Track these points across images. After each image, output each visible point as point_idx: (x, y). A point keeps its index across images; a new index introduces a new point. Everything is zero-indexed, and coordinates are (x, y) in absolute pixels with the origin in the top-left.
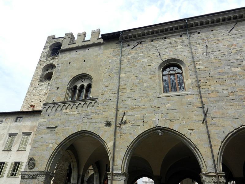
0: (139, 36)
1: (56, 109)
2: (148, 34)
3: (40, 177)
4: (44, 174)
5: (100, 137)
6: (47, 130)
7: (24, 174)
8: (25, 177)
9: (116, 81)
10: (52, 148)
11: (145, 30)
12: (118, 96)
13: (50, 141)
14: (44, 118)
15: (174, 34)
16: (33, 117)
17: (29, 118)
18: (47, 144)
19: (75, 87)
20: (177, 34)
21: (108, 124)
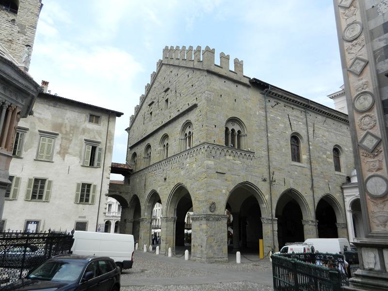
0: (279, 96)
2: (285, 98)
4: (226, 218)
6: (216, 174)
9: (265, 139)
12: (269, 155)
13: (222, 187)
15: (298, 108)
16: (54, 107)
17: (47, 106)
19: (227, 129)
20: (300, 109)
21: (265, 180)
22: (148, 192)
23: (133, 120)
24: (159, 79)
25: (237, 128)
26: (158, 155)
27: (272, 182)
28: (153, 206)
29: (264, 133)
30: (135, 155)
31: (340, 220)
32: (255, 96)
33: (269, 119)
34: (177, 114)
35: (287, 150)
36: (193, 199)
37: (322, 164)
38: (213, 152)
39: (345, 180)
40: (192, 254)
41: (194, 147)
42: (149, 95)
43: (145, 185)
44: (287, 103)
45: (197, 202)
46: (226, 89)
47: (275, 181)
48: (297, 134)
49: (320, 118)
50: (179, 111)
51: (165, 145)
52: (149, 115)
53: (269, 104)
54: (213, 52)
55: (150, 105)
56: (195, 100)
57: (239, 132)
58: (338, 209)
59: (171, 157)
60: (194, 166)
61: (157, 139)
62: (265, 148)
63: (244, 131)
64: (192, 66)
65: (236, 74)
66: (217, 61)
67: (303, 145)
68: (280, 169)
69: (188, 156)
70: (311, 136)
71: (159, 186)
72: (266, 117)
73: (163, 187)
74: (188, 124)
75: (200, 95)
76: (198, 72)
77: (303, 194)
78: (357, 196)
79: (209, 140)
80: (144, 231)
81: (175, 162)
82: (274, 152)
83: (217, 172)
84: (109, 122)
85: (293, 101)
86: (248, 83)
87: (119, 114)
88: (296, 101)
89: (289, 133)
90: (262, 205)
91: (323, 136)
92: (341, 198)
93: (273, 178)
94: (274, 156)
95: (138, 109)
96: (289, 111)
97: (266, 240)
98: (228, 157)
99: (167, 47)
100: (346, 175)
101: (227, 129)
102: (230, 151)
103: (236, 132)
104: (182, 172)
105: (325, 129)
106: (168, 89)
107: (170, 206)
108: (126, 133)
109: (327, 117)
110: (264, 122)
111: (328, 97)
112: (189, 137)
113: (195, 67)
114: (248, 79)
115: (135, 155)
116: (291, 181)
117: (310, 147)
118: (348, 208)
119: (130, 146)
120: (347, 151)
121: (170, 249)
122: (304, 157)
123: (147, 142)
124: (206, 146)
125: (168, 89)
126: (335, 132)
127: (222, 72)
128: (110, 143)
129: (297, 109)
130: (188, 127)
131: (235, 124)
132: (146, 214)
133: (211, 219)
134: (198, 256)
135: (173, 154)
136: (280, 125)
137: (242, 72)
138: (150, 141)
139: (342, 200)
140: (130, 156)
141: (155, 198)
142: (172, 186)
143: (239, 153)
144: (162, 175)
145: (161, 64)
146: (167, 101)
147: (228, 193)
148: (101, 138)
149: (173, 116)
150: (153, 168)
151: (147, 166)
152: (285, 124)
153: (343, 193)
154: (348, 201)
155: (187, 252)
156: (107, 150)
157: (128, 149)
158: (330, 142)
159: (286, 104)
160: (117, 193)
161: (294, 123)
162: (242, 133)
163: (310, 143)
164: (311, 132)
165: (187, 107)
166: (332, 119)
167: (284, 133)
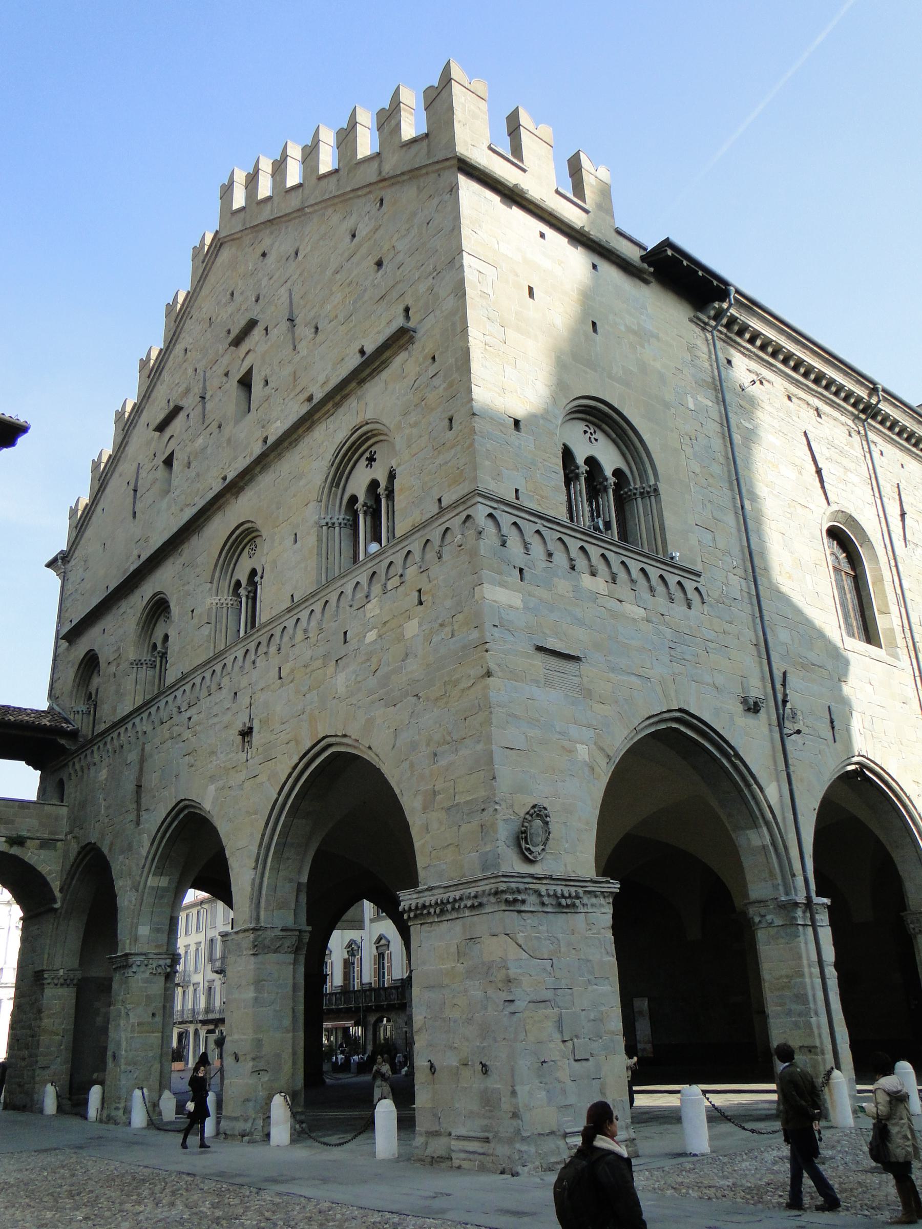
1: (550, 555)
3: (592, 905)
5: (737, 755)
7: (522, 886)
8: (523, 902)
9: (730, 520)
13: (574, 731)
15: (836, 414)
18: (566, 744)
19: (567, 455)
20: (843, 419)
21: (753, 708)
22: (156, 814)
24: (205, 307)
25: (610, 459)
26: (206, 630)
29: (723, 495)
30: (90, 664)
40: (423, 1123)
41: (405, 537)
43: (139, 787)
44: (796, 383)
47: (794, 715)
48: (851, 520)
50: (310, 399)
52: (161, 472)
55: (161, 427)
57: (617, 473)
61: (200, 560)
62: (736, 560)
63: (643, 475)
67: (878, 569)
71: (212, 779)
74: (361, 446)
75: (422, 288)
80: (133, 1020)
81: (300, 635)
83: (540, 649)
93: (785, 702)
98: (586, 580)
101: (567, 455)
102: (594, 552)
104: (341, 681)
106: (252, 324)
107: (276, 870)
108: (53, 580)
110: (717, 444)
115: (90, 664)
121: (279, 1107)
124: (480, 512)
125: (252, 324)
129: (835, 419)
130: (363, 462)
131: (599, 435)
132: (144, 931)
133: (532, 902)
134: (463, 1131)
138: (163, 580)
140: (70, 674)
141: (195, 853)
144: (227, 718)
146: (246, 383)
150: (181, 698)
151: (148, 697)
155: (385, 1111)
159: (793, 389)
162: (635, 484)
167: (800, 510)
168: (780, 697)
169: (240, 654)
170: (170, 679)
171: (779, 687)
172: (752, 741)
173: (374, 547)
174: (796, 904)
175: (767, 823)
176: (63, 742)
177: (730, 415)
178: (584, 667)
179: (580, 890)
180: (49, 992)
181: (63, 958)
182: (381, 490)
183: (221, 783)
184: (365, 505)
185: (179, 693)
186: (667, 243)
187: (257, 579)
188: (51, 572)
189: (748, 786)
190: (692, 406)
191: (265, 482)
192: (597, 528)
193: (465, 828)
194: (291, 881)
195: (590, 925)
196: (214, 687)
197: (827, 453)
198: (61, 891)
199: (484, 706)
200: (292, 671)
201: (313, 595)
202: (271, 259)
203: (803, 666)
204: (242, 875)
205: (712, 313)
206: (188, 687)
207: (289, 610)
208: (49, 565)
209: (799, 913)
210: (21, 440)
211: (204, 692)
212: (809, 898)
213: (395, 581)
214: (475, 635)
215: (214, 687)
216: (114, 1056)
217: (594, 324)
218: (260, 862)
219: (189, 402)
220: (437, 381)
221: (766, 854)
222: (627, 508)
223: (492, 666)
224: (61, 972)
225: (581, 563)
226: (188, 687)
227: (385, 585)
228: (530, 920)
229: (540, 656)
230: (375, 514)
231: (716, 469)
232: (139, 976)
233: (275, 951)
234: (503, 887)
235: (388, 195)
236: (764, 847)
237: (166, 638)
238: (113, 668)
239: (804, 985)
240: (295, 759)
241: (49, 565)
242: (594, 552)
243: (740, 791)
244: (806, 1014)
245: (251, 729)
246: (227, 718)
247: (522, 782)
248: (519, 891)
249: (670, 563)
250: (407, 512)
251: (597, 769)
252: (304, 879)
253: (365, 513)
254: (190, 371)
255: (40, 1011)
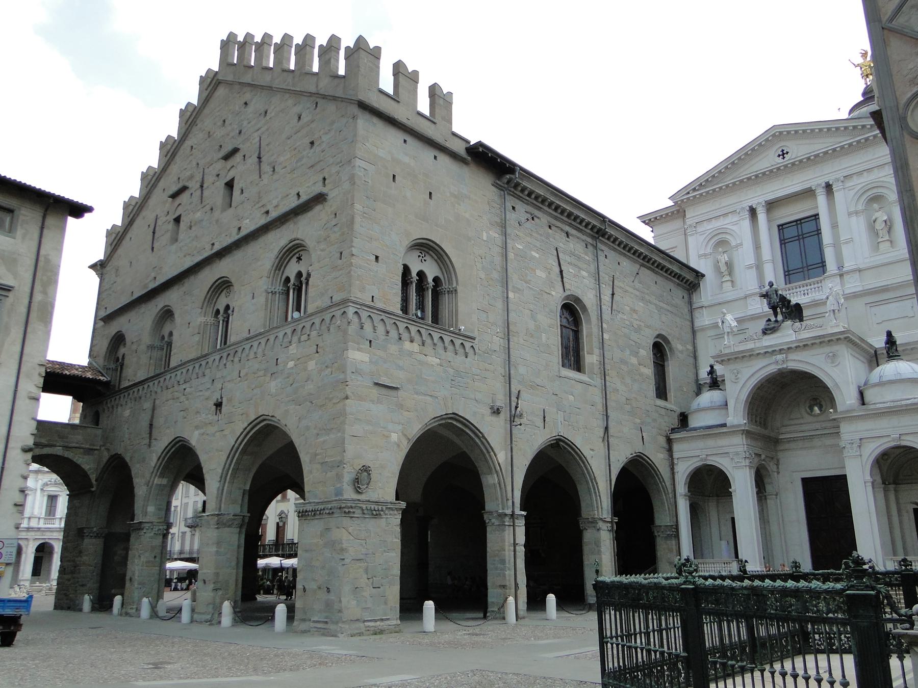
1: (388, 332)
5: (483, 436)
6: (375, 391)
9: (500, 305)
10: (399, 446)
11: (552, 193)
14: (358, 350)
15: (579, 235)
19: (406, 270)
20: (584, 237)
21: (496, 412)
22: (162, 442)
23: (116, 239)
24: (207, 122)
25: (431, 271)
27: (514, 418)
28: (173, 488)
30: (119, 340)
31: (662, 519)
32: (478, 186)
33: (511, 255)
34: (263, 221)
35: (553, 339)
36: (304, 458)
37: (628, 380)
38: (368, 327)
39: (675, 422)
40: (298, 615)
41: (312, 315)
42: (174, 169)
43: (151, 425)
44: (556, 218)
45: (319, 466)
46: (406, 160)
47: (521, 416)
48: (578, 300)
49: (628, 265)
50: (267, 212)
51: (218, 312)
52: (171, 226)
53: (512, 217)
54: (376, 54)
55: (174, 196)
56: (321, 183)
57: (436, 280)
58: (659, 491)
59: (241, 342)
60: (312, 365)
63: (450, 282)
64: (313, 89)
65: (433, 125)
66: (386, 82)
67: (589, 330)
68: (534, 387)
69: (295, 339)
70: (606, 308)
71: (197, 427)
72: (505, 247)
73: (211, 430)
74: (295, 250)
75: (334, 169)
76: (331, 107)
77: (586, 452)
78: (702, 460)
79: (359, 295)
80: (143, 559)
81: (252, 355)
82: (522, 341)
84: (42, 228)
85: (570, 215)
86: (462, 152)
87: (78, 210)
88: (576, 217)
89: (557, 297)
90: (489, 477)
91: (635, 311)
92: (667, 463)
93: (516, 407)
94: (522, 352)
95: (134, 210)
96: (559, 240)
97: (496, 569)
98: (407, 345)
99: (232, 36)
100: (679, 411)
101: (406, 270)
102: (413, 329)
103: (430, 279)
104: (273, 386)
105: (638, 293)
106: (235, 151)
107: (232, 482)
108: (94, 280)
109: (642, 265)
110: (498, 260)
111: (639, 221)
112: (297, 288)
113: (321, 92)
114: (464, 145)
115: (119, 340)
116: (560, 417)
117: (606, 336)
118: (682, 488)
119: (103, 314)
120: (681, 352)
121: (227, 606)
122: (590, 359)
123: (160, 302)
125: (235, 151)
126: (658, 303)
127: (399, 113)
128: (45, 293)
130: (294, 259)
131: (428, 258)
132: (151, 509)
134: (316, 619)
135: (246, 335)
136: (539, 273)
137: (450, 121)
138: (171, 298)
139: (668, 469)
140: (104, 344)
141: (184, 464)
142: (240, 426)
143: (436, 336)
144: (207, 394)
145: (211, 84)
146: (230, 185)
147: (405, 448)
148: (15, 275)
149: (249, 226)
150: (180, 375)
151: (158, 372)
152: (549, 271)
153: (670, 450)
154: (683, 470)
156: (33, 315)
157: (95, 323)
158: (648, 327)
160: (58, 451)
161: (568, 270)
162: (445, 286)
163: (604, 325)
164: (606, 298)
165: (293, 203)
166: (653, 271)
168: (514, 405)
169: (217, 358)
170: (173, 364)
171: (514, 399)
172: (493, 431)
173: (296, 315)
174: (506, 515)
175: (497, 472)
176: (100, 388)
177: (508, 241)
178: (400, 393)
179: (384, 508)
180: (87, 541)
181: (96, 520)
182: (303, 279)
183: (202, 431)
184: (294, 285)
185: (179, 373)
186: (480, 144)
187: (230, 312)
188: (92, 273)
189: (488, 452)
190: (485, 238)
191: (238, 256)
192: (417, 316)
193: (329, 474)
194: (240, 489)
195: (388, 524)
196: (200, 374)
197: (568, 258)
198: (96, 480)
199: (343, 413)
200: (247, 374)
201: (260, 334)
202: (250, 109)
203: (531, 387)
204: (212, 481)
205: (506, 181)
206: (184, 371)
207: (247, 339)
208: (92, 267)
209: (507, 519)
210: (87, 215)
211: (195, 376)
212: (513, 512)
213: (304, 337)
214: (342, 376)
215: (200, 374)
216: (131, 579)
217: (430, 193)
218: (223, 478)
219: (194, 185)
220: (336, 229)
221: (495, 488)
222: (440, 298)
223: (349, 393)
224: (95, 529)
225: (405, 335)
226: (184, 371)
227: (299, 339)
228: (357, 521)
229: (377, 387)
230: (299, 290)
231: (495, 275)
232: (148, 535)
233: (229, 526)
234: (343, 505)
235: (321, 102)
236: (494, 484)
237: (171, 334)
238: (134, 347)
239: (505, 555)
240: (246, 425)
241: (92, 267)
242: (413, 329)
243: (484, 455)
244: (504, 569)
245: (221, 403)
246: (207, 394)
247: (357, 454)
248: (352, 507)
249: (459, 334)
250: (314, 299)
251: (401, 446)
252: (248, 488)
253: (294, 289)
254: (194, 164)
255: (80, 552)
